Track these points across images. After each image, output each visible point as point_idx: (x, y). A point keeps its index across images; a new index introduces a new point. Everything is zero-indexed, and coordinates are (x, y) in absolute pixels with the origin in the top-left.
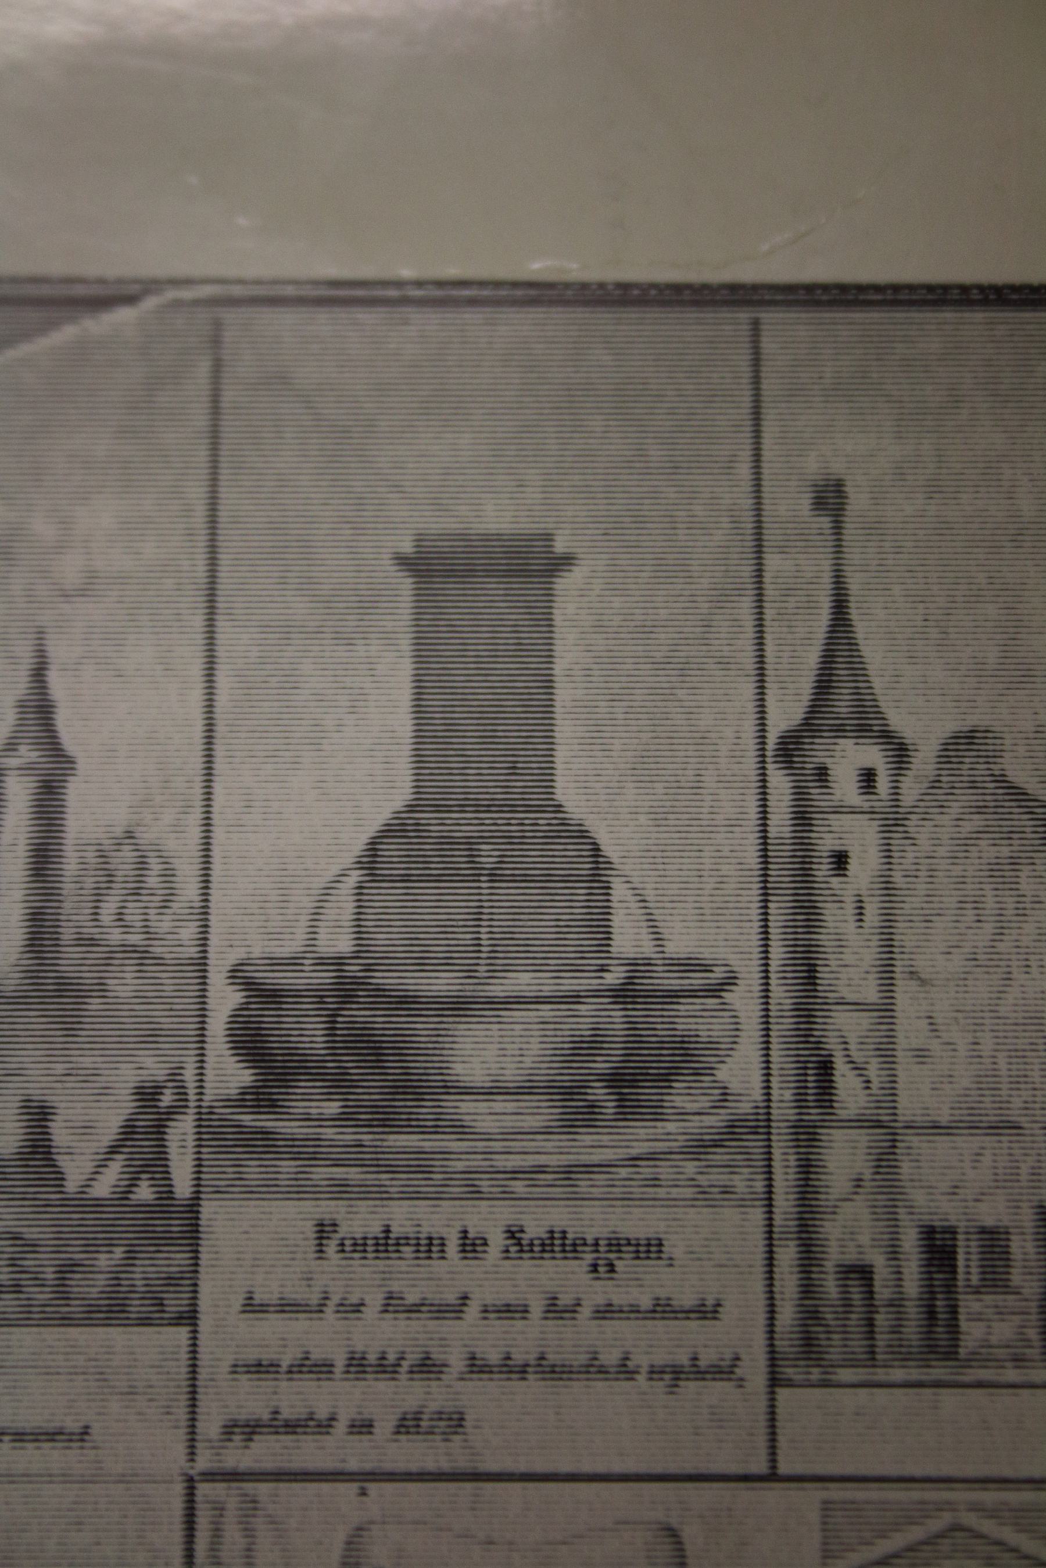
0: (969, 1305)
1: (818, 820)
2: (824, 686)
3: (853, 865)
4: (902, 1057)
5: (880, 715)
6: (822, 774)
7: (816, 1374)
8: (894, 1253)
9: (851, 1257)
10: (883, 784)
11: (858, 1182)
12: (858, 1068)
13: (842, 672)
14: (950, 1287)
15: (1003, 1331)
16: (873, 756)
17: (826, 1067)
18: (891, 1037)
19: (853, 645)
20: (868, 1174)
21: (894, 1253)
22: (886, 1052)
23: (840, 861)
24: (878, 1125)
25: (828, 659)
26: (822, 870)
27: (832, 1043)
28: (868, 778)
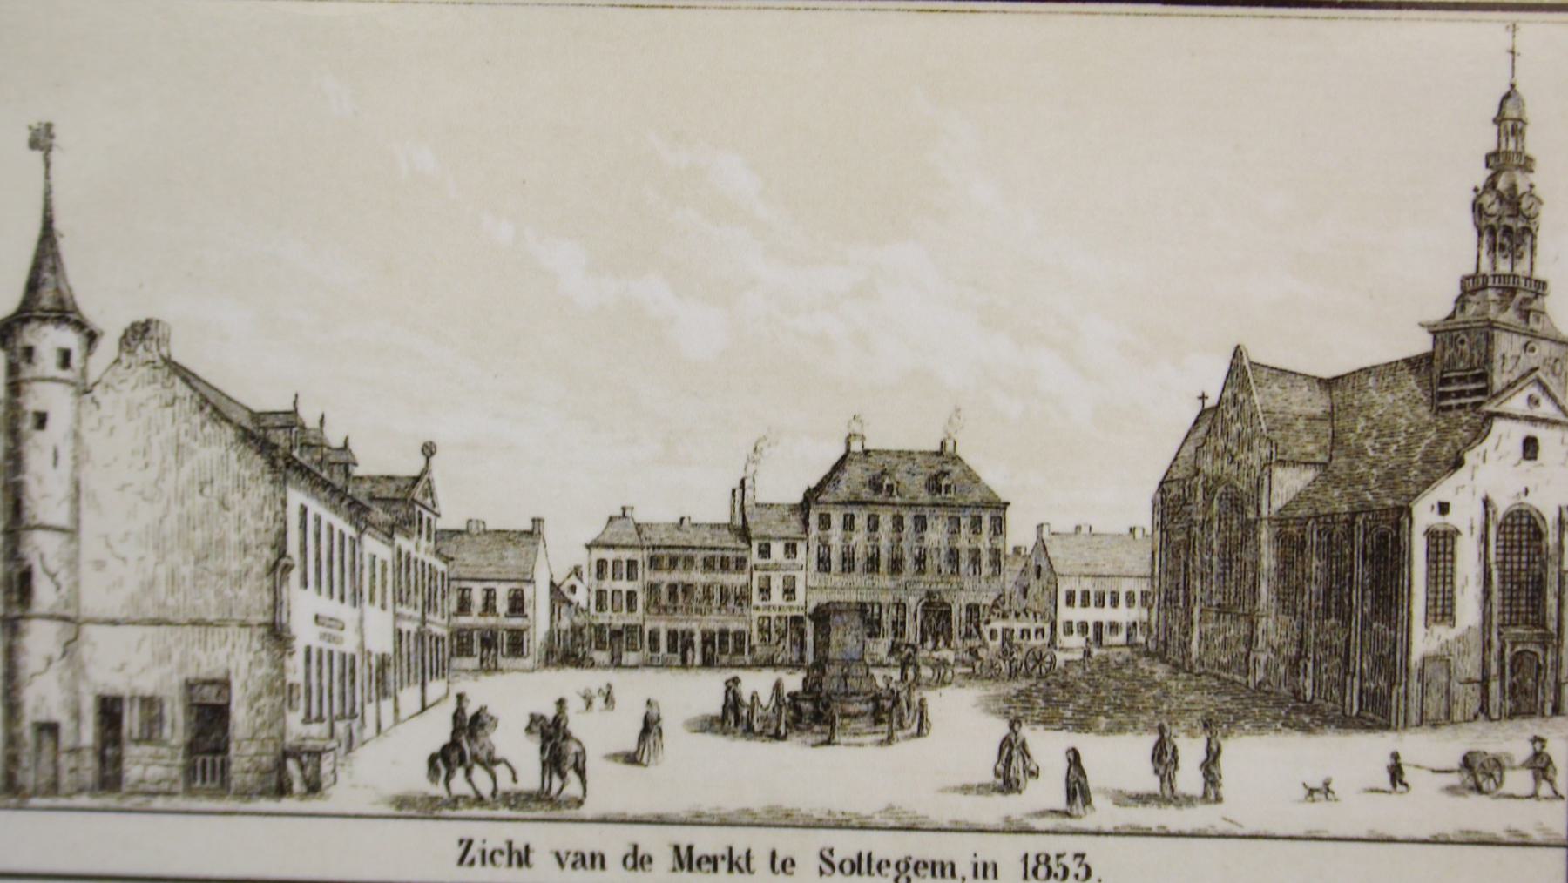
0: (132, 752)
1: (25, 387)
2: (33, 286)
3: (51, 423)
4: (86, 570)
5: (75, 310)
6: (29, 352)
7: (13, 801)
8: (77, 716)
9: (42, 717)
10: (76, 359)
11: (49, 661)
12: (53, 576)
13: (46, 275)
14: (117, 741)
15: (156, 771)
16: (69, 338)
17: (26, 577)
18: (77, 553)
19: (56, 256)
20: (58, 652)
21: (77, 716)
22: (73, 563)
23: (41, 420)
24: (65, 619)
25: (37, 267)
26: (27, 425)
27: (34, 560)
28: (65, 358)
